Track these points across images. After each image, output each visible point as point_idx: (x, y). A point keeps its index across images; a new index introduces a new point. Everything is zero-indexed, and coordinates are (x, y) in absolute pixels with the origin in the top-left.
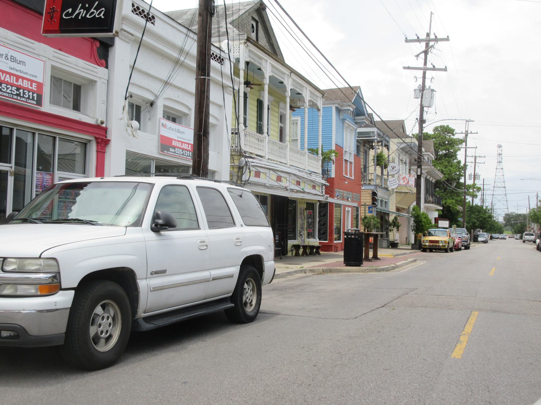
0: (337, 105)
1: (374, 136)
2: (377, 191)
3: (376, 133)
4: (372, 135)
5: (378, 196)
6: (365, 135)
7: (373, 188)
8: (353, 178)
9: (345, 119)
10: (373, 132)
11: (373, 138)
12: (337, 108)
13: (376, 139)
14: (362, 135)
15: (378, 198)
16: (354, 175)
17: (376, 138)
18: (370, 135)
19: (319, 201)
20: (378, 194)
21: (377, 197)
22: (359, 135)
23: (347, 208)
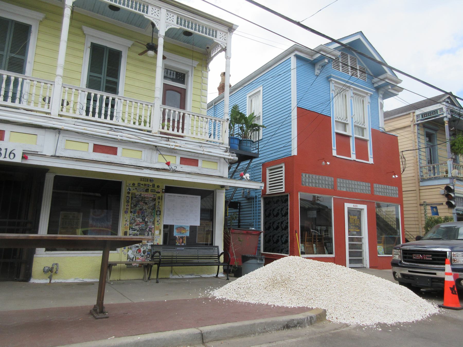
0: (297, 53)
1: (443, 114)
2: (453, 186)
3: (445, 110)
4: (439, 113)
5: (455, 192)
6: (431, 115)
7: (447, 182)
8: (371, 161)
9: (330, 77)
10: (441, 109)
11: (441, 116)
12: (298, 57)
13: (446, 117)
14: (427, 116)
15: (456, 195)
16: (374, 158)
17: (445, 115)
18: (437, 113)
19: (222, 187)
20: (455, 189)
21: (454, 194)
22: (423, 117)
23: (347, 206)
